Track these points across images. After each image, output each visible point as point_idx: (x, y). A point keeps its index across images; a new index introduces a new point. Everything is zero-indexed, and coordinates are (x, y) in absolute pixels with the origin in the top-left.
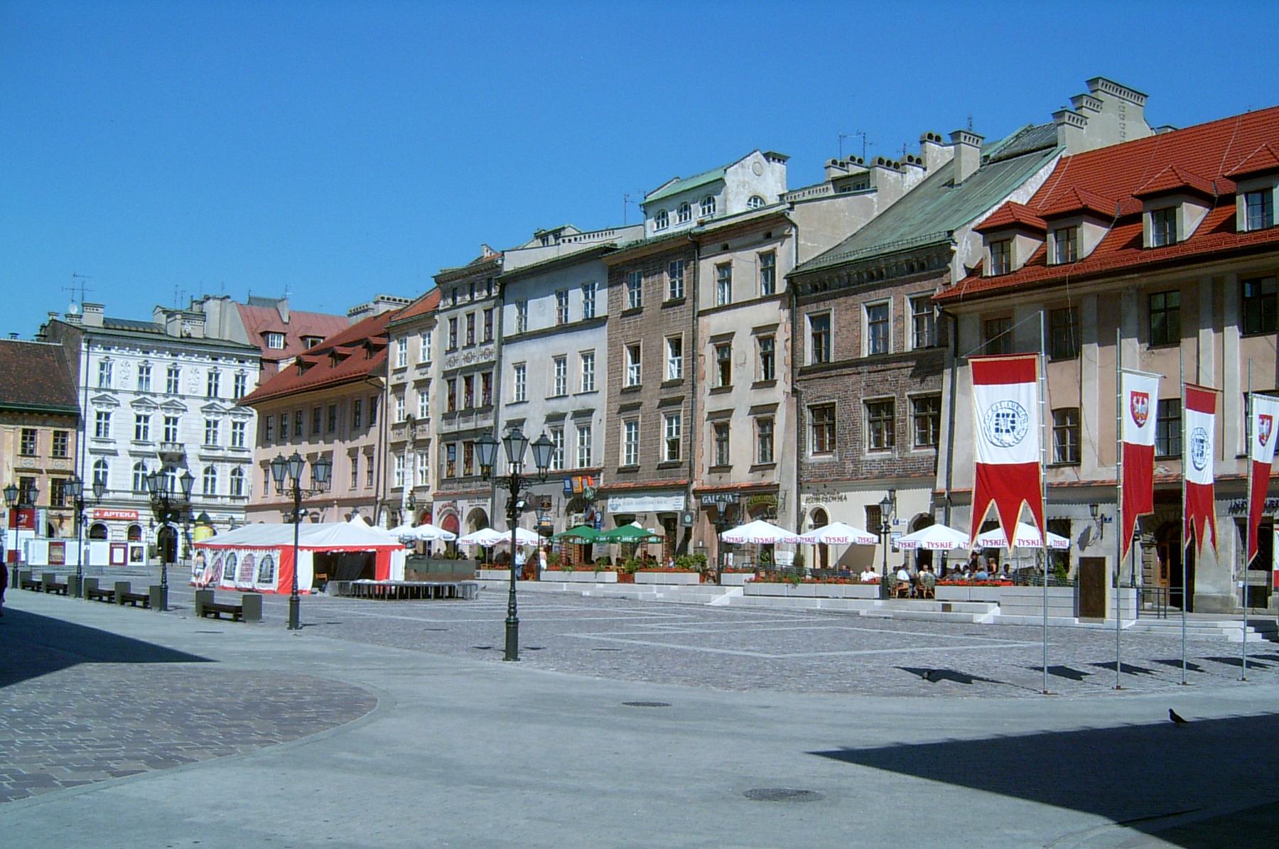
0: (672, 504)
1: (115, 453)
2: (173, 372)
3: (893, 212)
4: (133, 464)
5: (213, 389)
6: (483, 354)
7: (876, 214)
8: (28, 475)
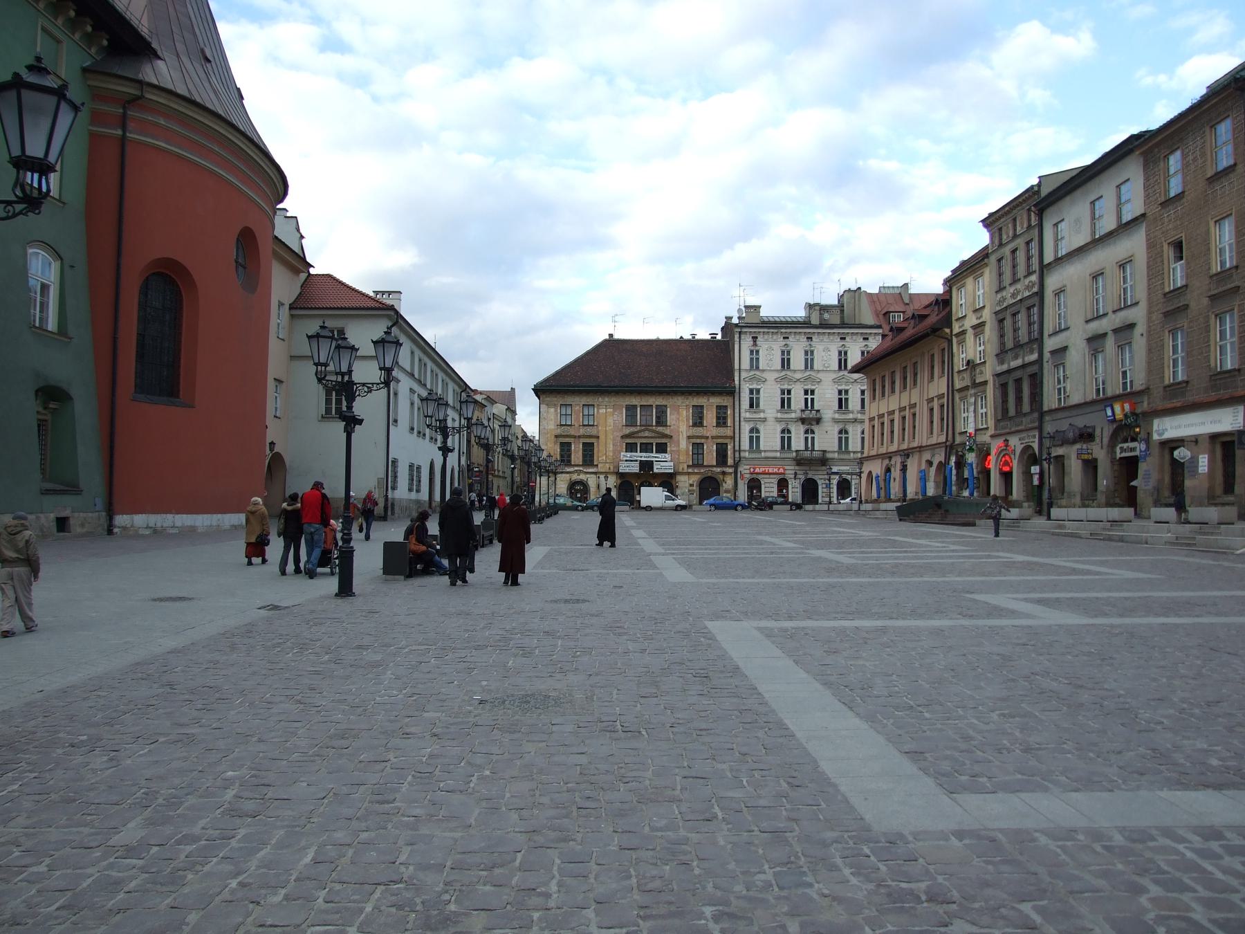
1: (764, 420)
2: (809, 354)
4: (779, 429)
5: (842, 364)
8: (698, 441)
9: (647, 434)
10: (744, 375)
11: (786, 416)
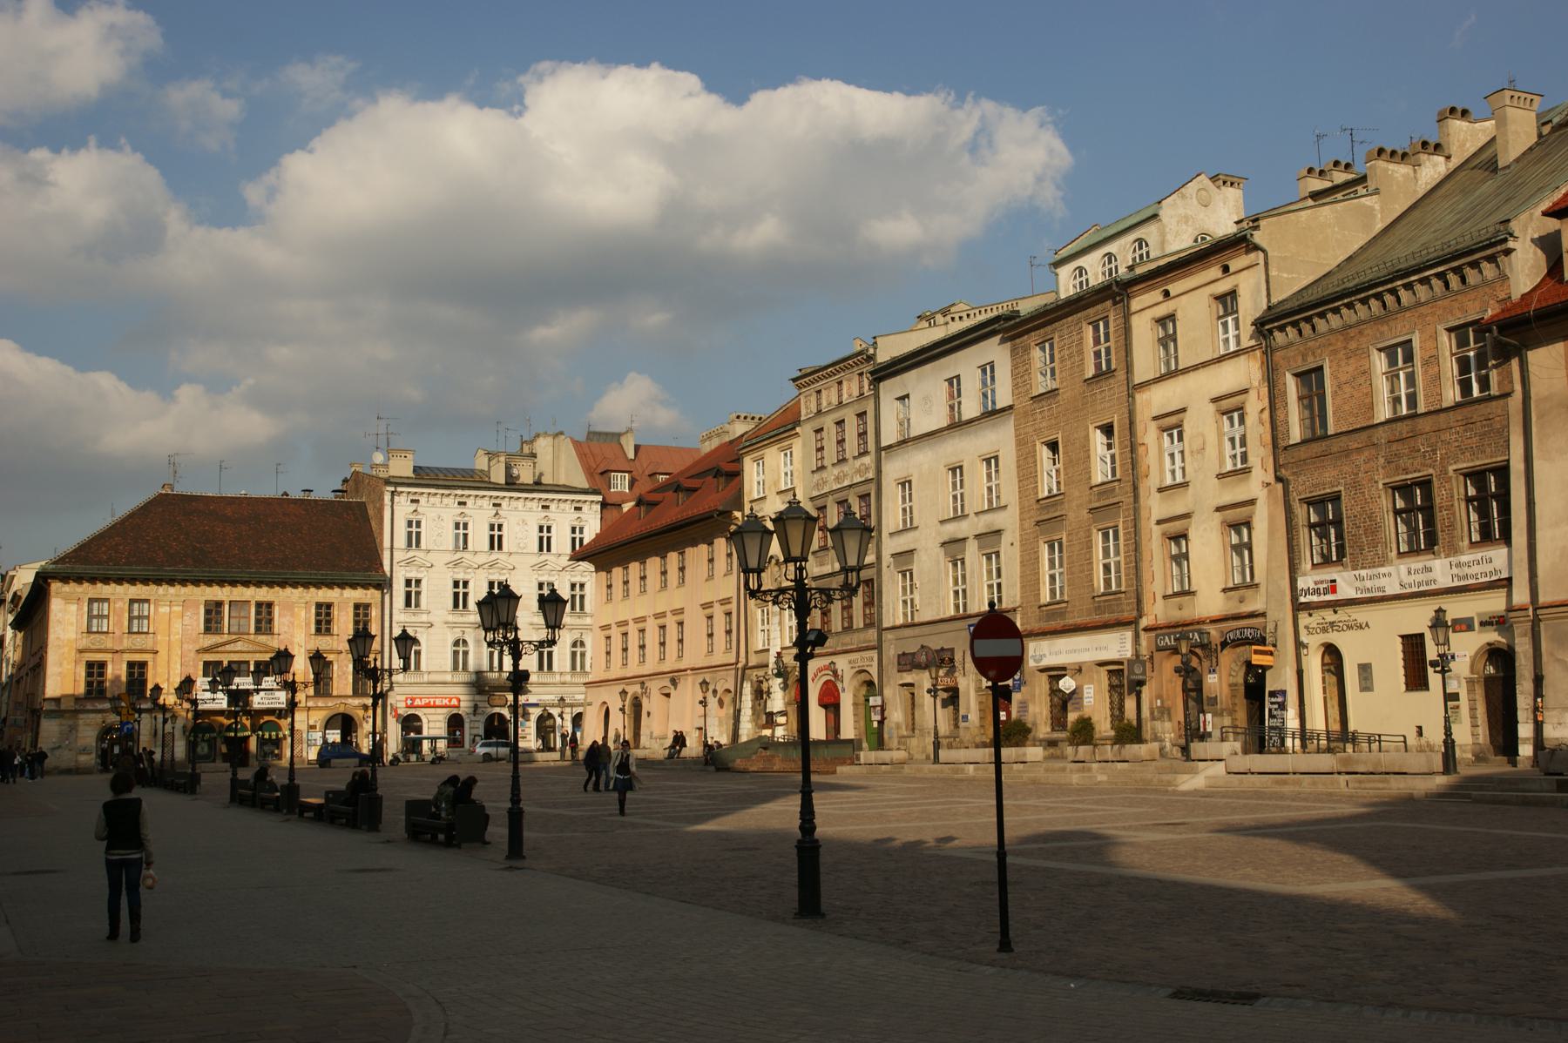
0: (1116, 646)
3: (1403, 222)
4: (450, 641)
5: (544, 545)
6: (858, 471)
7: (1379, 227)
9: (239, 646)
10: (398, 556)
11: (461, 619)
